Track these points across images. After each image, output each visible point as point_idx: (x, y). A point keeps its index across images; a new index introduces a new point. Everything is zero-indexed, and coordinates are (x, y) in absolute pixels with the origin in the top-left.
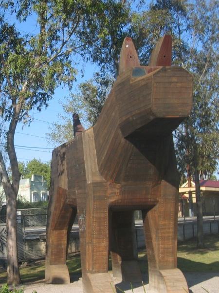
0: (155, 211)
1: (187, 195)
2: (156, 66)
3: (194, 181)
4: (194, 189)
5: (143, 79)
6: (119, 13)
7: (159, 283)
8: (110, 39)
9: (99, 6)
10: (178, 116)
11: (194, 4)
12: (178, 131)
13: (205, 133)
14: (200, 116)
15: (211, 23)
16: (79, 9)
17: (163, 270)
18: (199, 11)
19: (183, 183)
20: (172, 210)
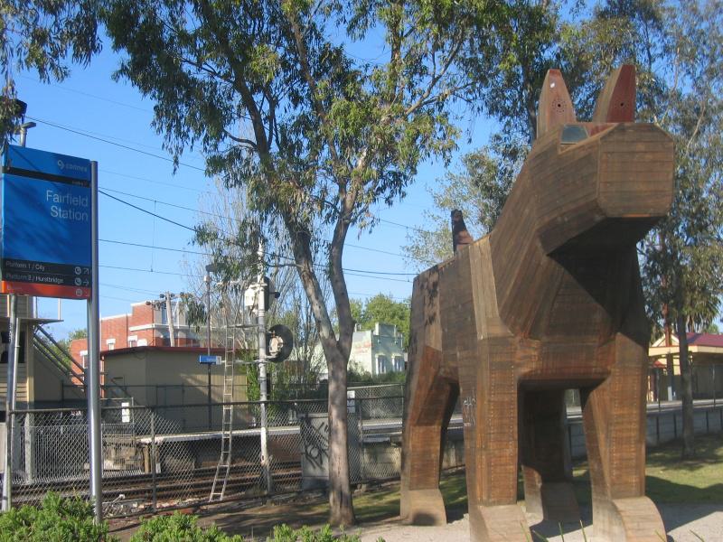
0: (604, 390)
1: (664, 361)
2: (607, 121)
3: (676, 334)
4: (677, 350)
5: (582, 147)
6: (537, 24)
7: (611, 523)
8: (521, 72)
9: (500, 11)
10: (647, 216)
11: (677, 7)
12: (647, 243)
13: (697, 247)
14: (688, 215)
15: (708, 42)
16: (464, 16)
17: (620, 500)
18: (686, 20)
19: (657, 339)
20: (637, 388)
